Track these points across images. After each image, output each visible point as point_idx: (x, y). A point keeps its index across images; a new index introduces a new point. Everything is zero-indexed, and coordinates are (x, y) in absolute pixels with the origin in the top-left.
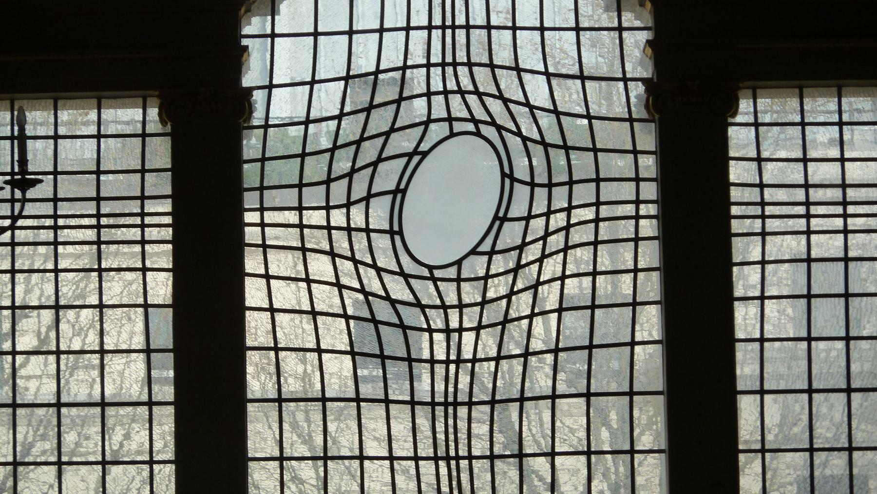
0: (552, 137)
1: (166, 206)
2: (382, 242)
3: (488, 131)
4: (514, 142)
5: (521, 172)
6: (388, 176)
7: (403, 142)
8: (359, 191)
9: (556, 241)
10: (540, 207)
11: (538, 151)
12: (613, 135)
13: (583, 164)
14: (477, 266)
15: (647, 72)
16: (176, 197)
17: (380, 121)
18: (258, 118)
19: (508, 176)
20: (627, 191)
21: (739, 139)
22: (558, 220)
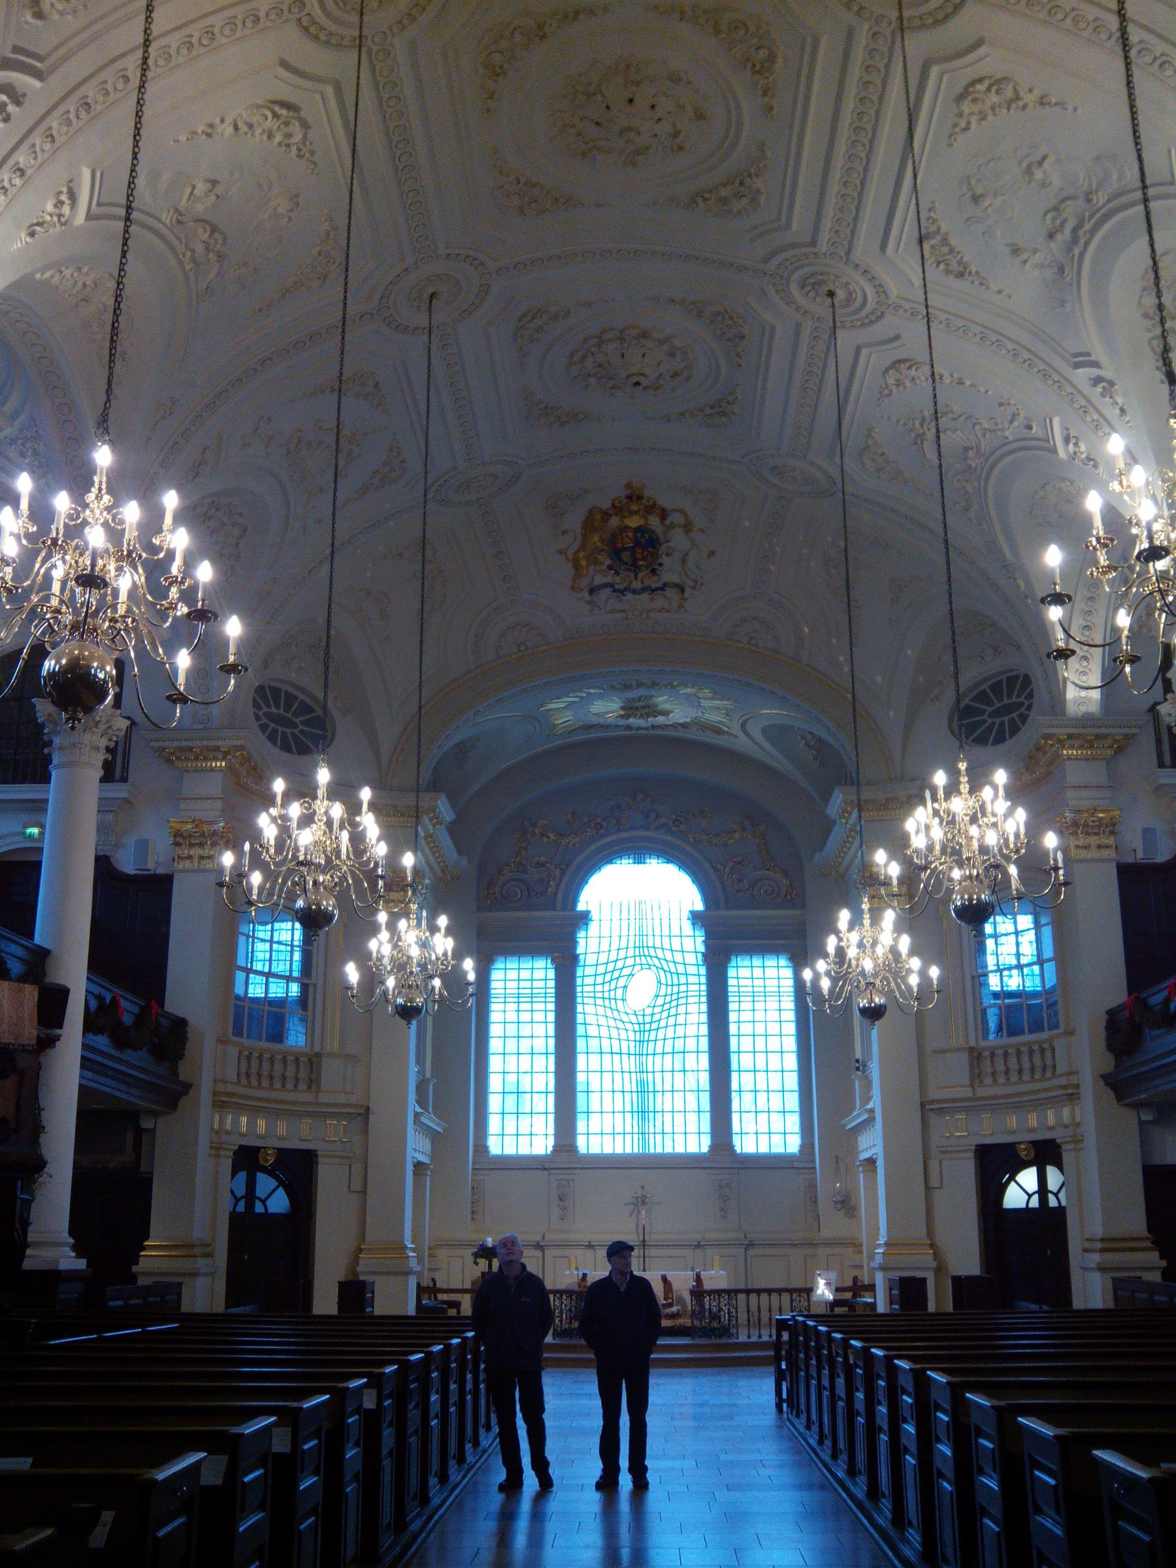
0: (673, 970)
1: (553, 991)
2: (620, 1003)
3: (653, 968)
4: (661, 972)
5: (663, 981)
6: (622, 982)
7: (626, 971)
8: (613, 986)
9: (674, 1003)
10: (669, 992)
11: (668, 975)
12: (692, 970)
13: (683, 979)
14: (649, 1011)
15: (703, 950)
16: (557, 988)
17: (620, 964)
18: (582, 963)
19: (659, 982)
20: (696, 987)
21: (731, 972)
22: (675, 997)
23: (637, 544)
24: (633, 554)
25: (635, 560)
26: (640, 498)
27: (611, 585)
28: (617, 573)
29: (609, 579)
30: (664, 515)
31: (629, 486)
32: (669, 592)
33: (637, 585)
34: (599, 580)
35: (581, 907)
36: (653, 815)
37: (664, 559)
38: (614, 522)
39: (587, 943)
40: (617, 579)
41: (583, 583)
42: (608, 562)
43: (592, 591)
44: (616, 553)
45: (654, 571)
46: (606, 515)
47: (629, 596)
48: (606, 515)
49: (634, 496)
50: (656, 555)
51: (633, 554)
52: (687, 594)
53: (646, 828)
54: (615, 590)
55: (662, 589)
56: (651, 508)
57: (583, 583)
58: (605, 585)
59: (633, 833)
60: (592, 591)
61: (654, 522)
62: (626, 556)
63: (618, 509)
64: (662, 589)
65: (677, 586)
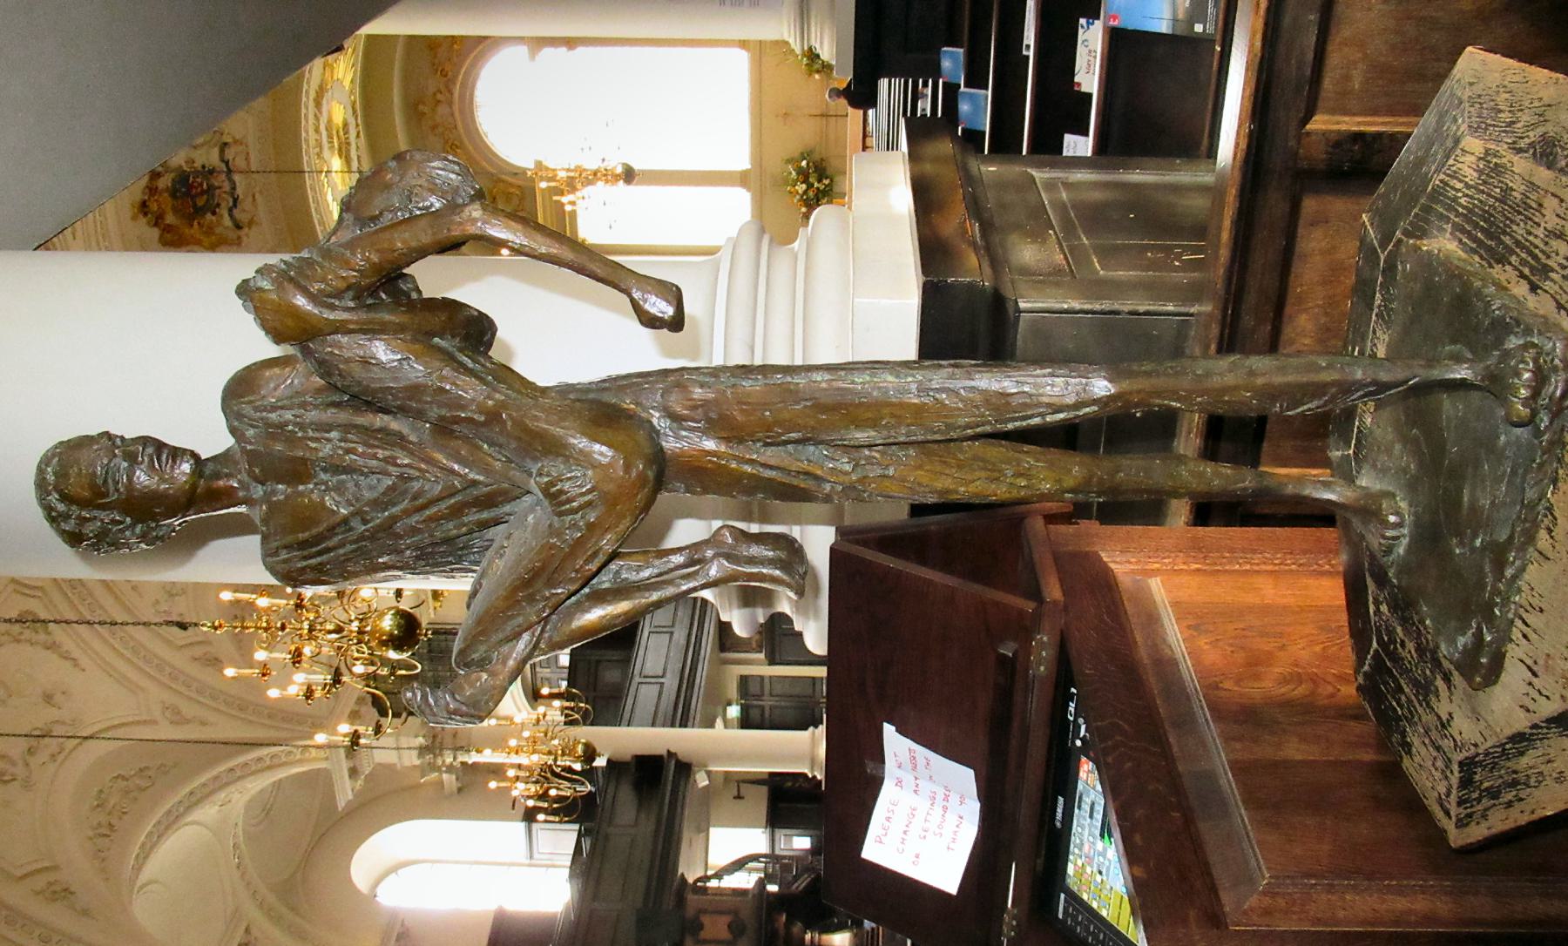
23: (188, 194)
24: (198, 195)
25: (203, 192)
26: (144, 204)
27: (230, 210)
28: (218, 205)
29: (226, 215)
30: (155, 175)
31: (134, 218)
32: (229, 154)
33: (227, 186)
34: (227, 222)
35: (532, 166)
36: (439, 96)
37: (198, 165)
38: (170, 219)
39: (560, 160)
40: (223, 205)
41: (232, 235)
42: (209, 216)
43: (238, 227)
44: (199, 212)
45: (211, 172)
46: (168, 229)
47: (239, 191)
48: (168, 229)
49: (143, 207)
50: (197, 173)
51: (198, 195)
52: (229, 140)
53: (450, 104)
54: (235, 205)
55: (227, 163)
56: (152, 190)
57: (232, 235)
58: (231, 216)
59: (457, 114)
60: (238, 227)
61: (165, 182)
62: (201, 202)
63: (158, 221)
64: (227, 163)
65: (222, 151)
